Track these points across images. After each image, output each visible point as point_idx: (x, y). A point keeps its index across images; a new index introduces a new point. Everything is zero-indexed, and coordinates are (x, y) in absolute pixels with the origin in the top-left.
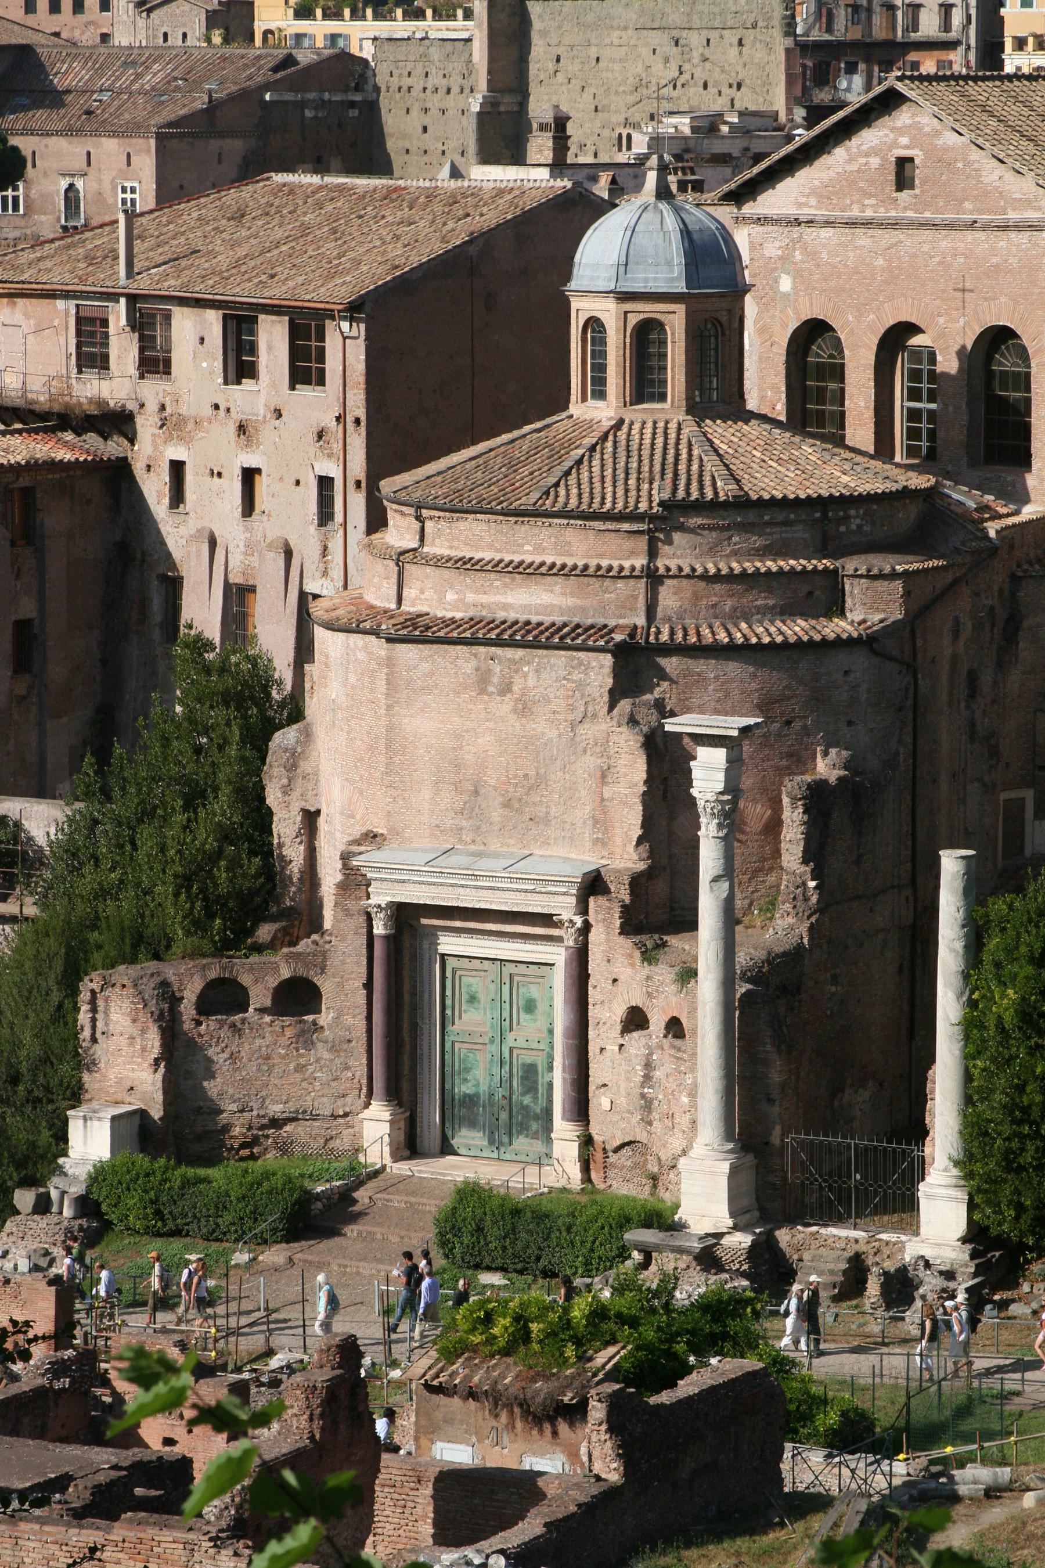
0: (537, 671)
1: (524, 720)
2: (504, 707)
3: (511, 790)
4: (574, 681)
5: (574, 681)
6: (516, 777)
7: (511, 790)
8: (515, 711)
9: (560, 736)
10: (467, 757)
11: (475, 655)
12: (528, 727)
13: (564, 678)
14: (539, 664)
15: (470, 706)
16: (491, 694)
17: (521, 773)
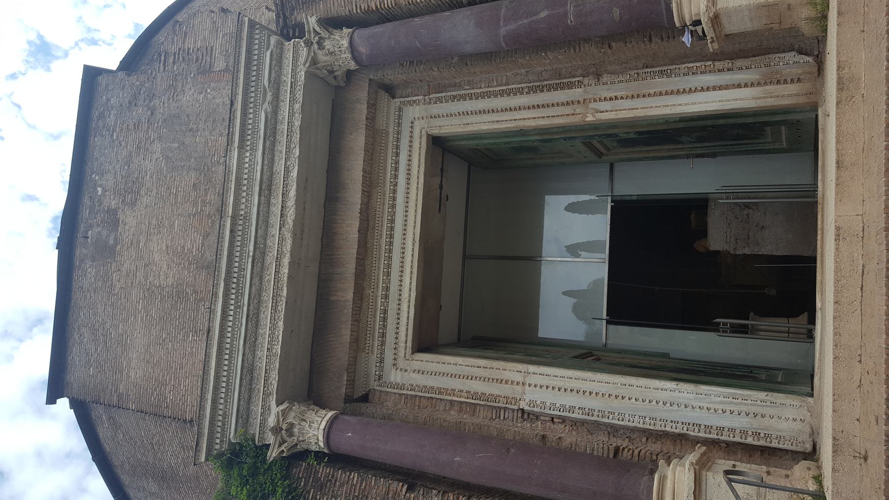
0: (102, 174)
1: (142, 192)
2: (130, 220)
3: (207, 209)
4: (115, 125)
5: (115, 125)
6: (195, 204)
7: (207, 209)
8: (133, 204)
9: (160, 138)
10: (170, 281)
11: (82, 261)
12: (148, 185)
13: (112, 135)
14: (97, 174)
15: (124, 273)
16: (116, 239)
17: (193, 194)
